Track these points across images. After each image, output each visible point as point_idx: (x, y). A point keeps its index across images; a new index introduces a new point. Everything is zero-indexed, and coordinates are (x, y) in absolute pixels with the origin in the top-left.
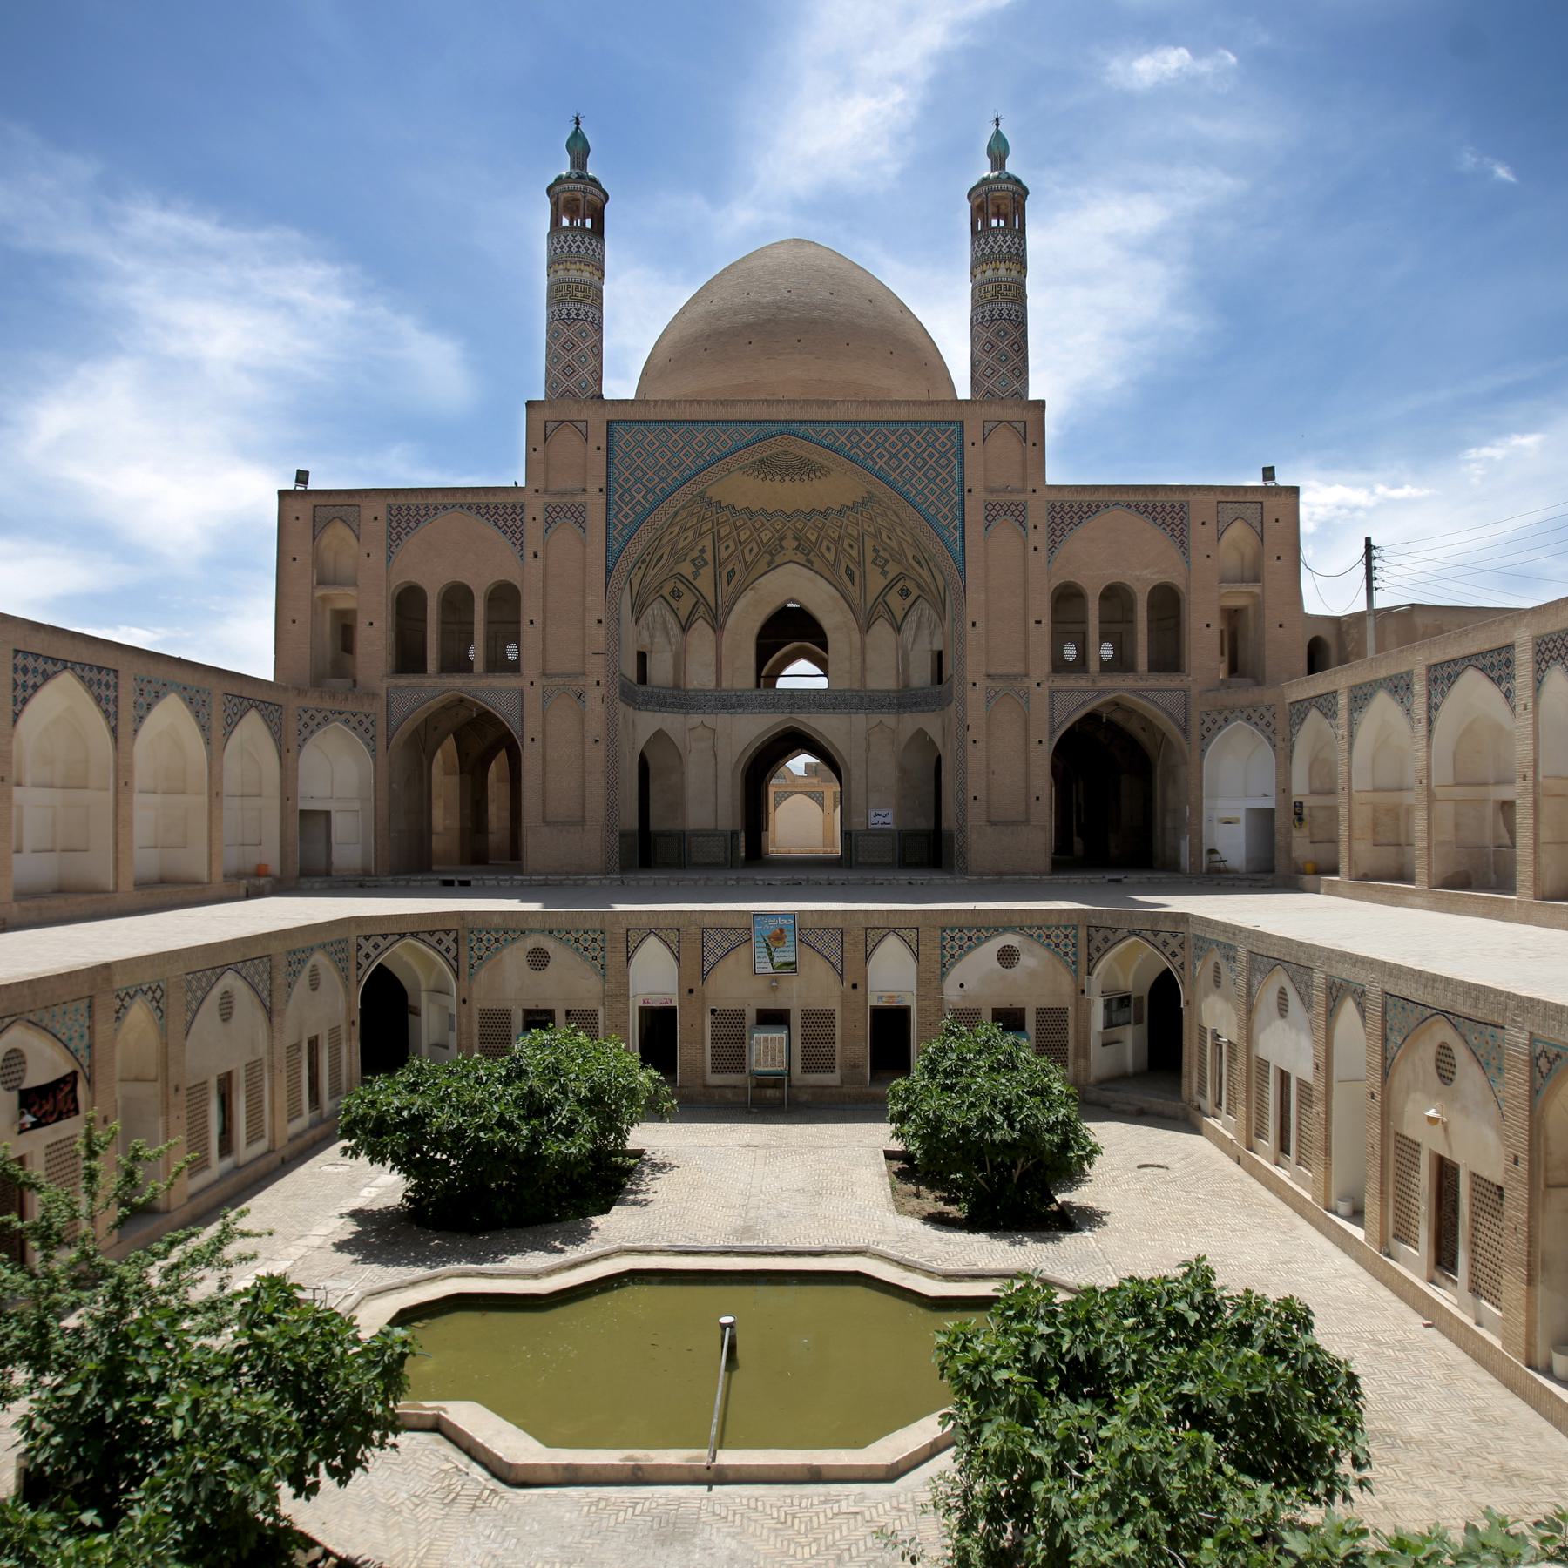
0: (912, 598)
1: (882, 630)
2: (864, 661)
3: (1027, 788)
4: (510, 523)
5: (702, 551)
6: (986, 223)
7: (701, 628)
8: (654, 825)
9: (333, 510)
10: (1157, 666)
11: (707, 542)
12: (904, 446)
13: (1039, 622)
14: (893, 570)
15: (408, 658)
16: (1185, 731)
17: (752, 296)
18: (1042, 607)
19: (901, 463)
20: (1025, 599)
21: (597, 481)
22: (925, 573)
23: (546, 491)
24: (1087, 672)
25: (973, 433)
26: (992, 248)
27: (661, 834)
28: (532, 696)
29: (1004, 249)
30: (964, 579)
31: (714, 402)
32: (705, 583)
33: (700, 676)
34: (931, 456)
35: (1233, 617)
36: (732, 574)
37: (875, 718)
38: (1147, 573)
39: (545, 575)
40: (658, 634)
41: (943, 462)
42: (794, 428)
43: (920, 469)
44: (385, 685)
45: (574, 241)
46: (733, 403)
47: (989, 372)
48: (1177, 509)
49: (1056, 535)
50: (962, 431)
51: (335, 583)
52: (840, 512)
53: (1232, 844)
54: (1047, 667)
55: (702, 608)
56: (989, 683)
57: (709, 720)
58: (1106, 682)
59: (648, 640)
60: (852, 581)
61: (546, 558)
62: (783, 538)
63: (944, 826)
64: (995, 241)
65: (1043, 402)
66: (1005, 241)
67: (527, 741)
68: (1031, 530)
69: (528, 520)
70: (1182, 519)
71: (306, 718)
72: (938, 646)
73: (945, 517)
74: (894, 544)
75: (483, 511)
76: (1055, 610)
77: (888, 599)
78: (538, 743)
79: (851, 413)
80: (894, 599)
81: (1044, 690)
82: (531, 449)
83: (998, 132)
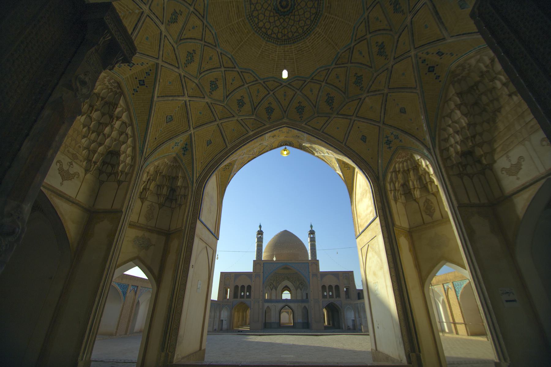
1: (299, 290)
7: (274, 290)
10: (336, 298)
18: (320, 289)
25: (310, 264)
33: (274, 298)
57: (275, 304)
80: (300, 286)
82: (254, 267)
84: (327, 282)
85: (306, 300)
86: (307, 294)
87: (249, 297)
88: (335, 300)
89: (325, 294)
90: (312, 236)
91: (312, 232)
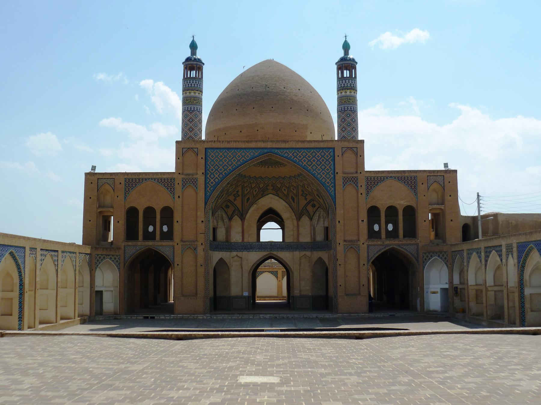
0: (316, 208)
1: (305, 220)
2: (298, 231)
3: (359, 281)
4: (169, 185)
5: (238, 192)
6: (342, 73)
7: (236, 218)
8: (218, 294)
9: (105, 180)
11: (240, 188)
12: (313, 157)
13: (363, 221)
14: (309, 198)
16: (417, 260)
17: (254, 89)
18: (364, 215)
19: (312, 163)
20: (358, 211)
22: (321, 201)
23: (183, 174)
24: (380, 238)
25: (338, 152)
26: (344, 84)
28: (178, 249)
29: (349, 85)
30: (335, 205)
31: (244, 141)
32: (238, 203)
33: (236, 237)
34: (323, 160)
35: (436, 216)
36: (248, 199)
37: (303, 253)
38: (402, 202)
39: (182, 204)
40: (220, 221)
42: (273, 150)
43: (319, 165)
44: (123, 244)
45: (193, 82)
46: (251, 142)
47: (344, 129)
48: (413, 179)
50: (334, 152)
51: (104, 207)
52: (290, 178)
53: (434, 302)
54: (366, 237)
55: (237, 212)
56: (345, 243)
57: (240, 254)
58: (387, 242)
59: (216, 224)
60: (293, 200)
61: (182, 198)
62: (268, 186)
63: (329, 294)
64: (346, 82)
65: (363, 141)
66: (349, 82)
67: (176, 265)
68: (359, 187)
70: (415, 182)
71: (98, 258)
72: (326, 225)
73: (328, 183)
74: (309, 190)
75: (160, 181)
76: (369, 216)
77: (307, 208)
78: (180, 266)
79: (294, 145)
80: (310, 208)
81: (365, 245)
82: (177, 158)
83: (346, 41)
84: (383, 198)
85: (327, 242)
86: (327, 229)
87: (168, 236)
88: (401, 244)
89: (376, 228)
90: (346, 73)
91: (346, 65)
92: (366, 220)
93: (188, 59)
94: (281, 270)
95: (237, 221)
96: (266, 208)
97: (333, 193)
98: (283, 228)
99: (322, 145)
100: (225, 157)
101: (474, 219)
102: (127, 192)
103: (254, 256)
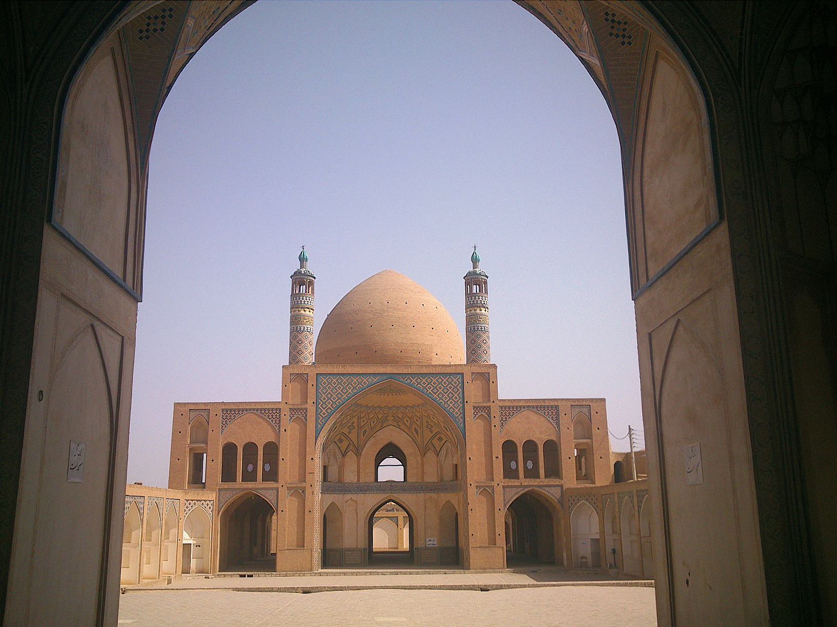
1: (431, 456)
10: (547, 476)
11: (355, 420)
14: (435, 430)
15: (228, 474)
16: (562, 505)
18: (498, 451)
21: (311, 399)
27: (332, 550)
28: (283, 492)
33: (350, 477)
37: (428, 495)
41: (455, 390)
49: (503, 422)
57: (354, 497)
60: (417, 433)
67: (280, 512)
69: (282, 415)
87: (271, 475)
89: (513, 464)
90: (475, 289)
92: (501, 457)
93: (297, 273)
94: (401, 515)
95: (351, 457)
96: (386, 443)
97: (462, 425)
98: (404, 464)
99: (449, 370)
100: (340, 383)
101: (627, 456)
102: (225, 424)
103: (371, 500)
